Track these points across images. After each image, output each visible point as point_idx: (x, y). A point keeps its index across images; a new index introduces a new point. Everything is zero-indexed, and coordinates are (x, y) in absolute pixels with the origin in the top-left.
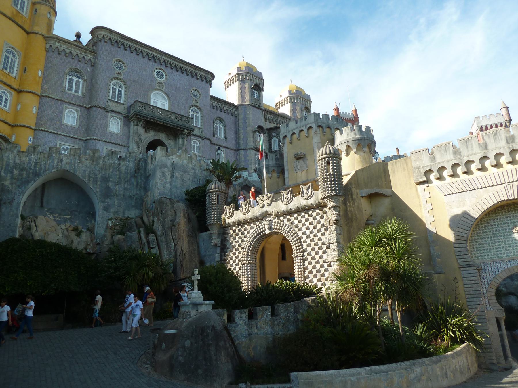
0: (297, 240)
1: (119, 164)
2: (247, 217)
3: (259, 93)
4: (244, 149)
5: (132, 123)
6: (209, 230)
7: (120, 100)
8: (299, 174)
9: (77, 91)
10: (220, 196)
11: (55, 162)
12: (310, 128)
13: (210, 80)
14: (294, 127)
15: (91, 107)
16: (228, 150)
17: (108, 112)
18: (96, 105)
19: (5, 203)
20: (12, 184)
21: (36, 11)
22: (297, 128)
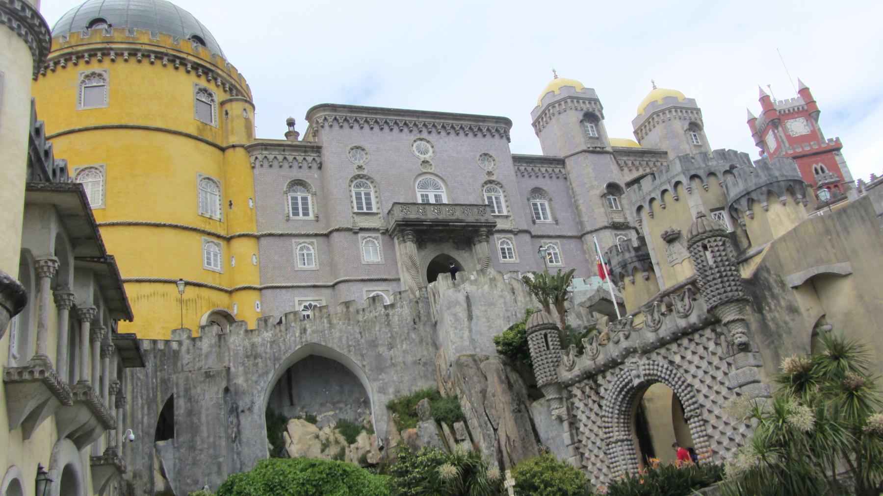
0: (686, 387)
1: (388, 315)
2: (597, 363)
3: (596, 126)
4: (592, 232)
5: (396, 239)
6: (543, 396)
7: (370, 208)
8: (678, 268)
9: (306, 214)
10: (549, 335)
11: (297, 335)
12: (678, 183)
13: (505, 132)
14: (651, 188)
15: (331, 232)
16: (565, 241)
17: (356, 233)
18: (337, 227)
19: (243, 411)
20: (246, 381)
21: (227, 114)
22: (654, 189)
